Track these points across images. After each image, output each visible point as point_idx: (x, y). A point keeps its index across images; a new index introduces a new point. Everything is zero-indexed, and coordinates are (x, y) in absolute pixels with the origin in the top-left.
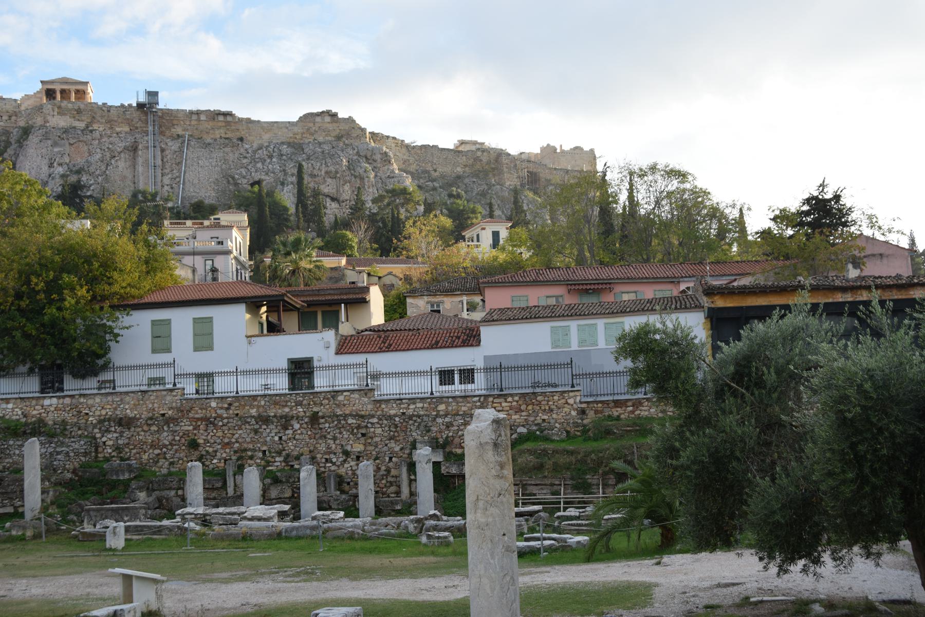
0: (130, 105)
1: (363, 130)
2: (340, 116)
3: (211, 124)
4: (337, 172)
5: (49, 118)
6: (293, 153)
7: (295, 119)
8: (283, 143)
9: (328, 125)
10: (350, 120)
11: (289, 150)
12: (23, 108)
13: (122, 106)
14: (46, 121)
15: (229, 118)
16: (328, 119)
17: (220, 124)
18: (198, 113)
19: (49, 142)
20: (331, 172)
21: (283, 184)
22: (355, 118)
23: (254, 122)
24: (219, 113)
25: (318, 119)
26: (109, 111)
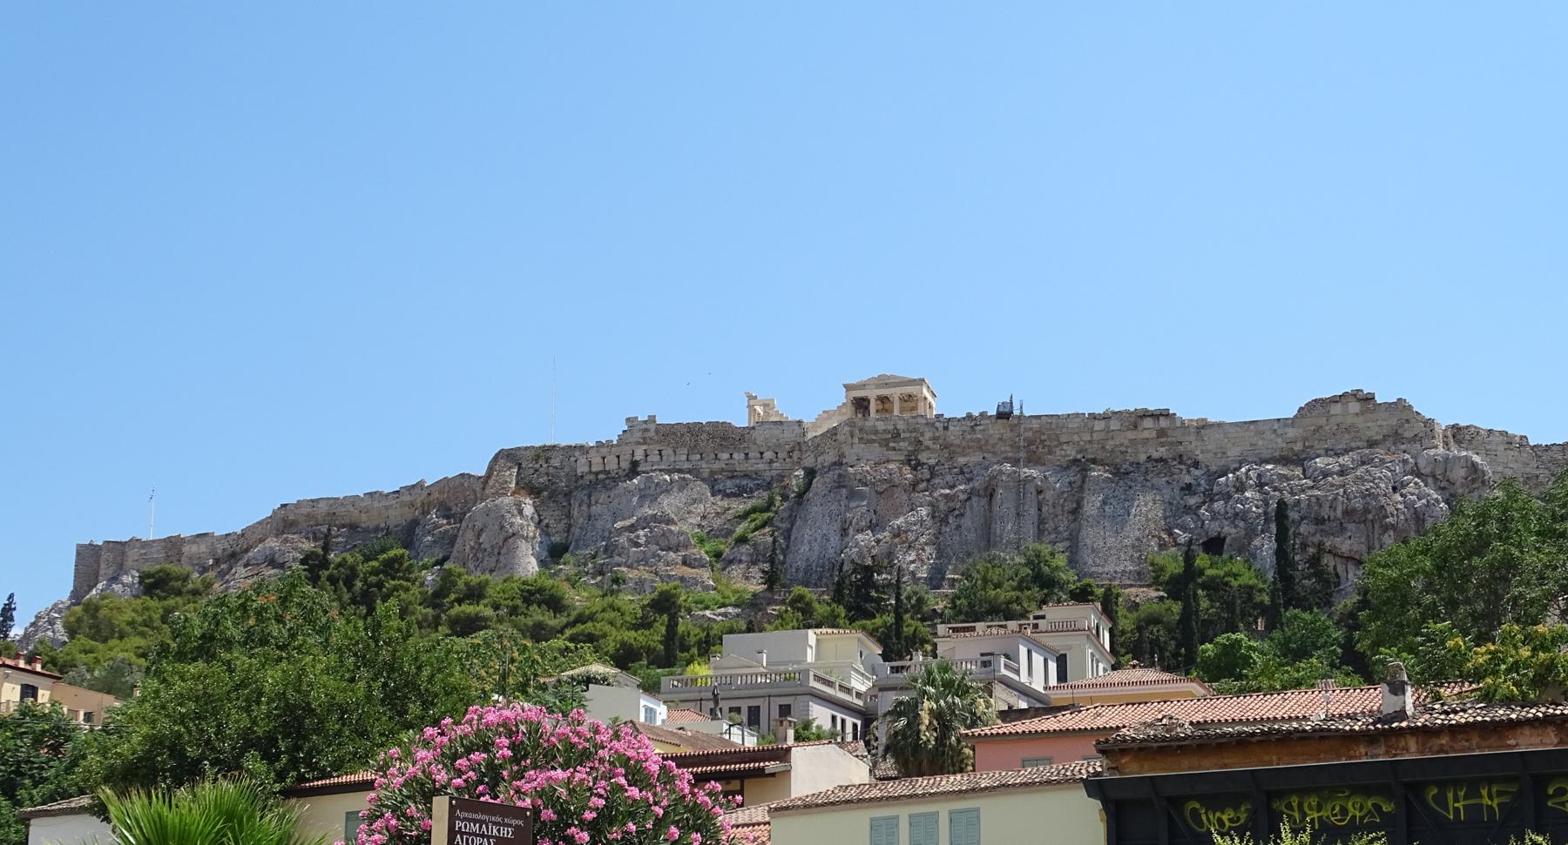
0: (983, 415)
1: (1429, 423)
3: (1131, 435)
4: (1366, 511)
5: (846, 450)
7: (1291, 413)
9: (1356, 420)
10: (1401, 406)
12: (810, 435)
13: (969, 416)
14: (842, 456)
15: (1163, 423)
16: (1354, 407)
17: (1146, 435)
18: (1106, 417)
19: (844, 491)
20: (1354, 510)
23: (1213, 425)
24: (1144, 415)
25: (1336, 409)
26: (946, 428)
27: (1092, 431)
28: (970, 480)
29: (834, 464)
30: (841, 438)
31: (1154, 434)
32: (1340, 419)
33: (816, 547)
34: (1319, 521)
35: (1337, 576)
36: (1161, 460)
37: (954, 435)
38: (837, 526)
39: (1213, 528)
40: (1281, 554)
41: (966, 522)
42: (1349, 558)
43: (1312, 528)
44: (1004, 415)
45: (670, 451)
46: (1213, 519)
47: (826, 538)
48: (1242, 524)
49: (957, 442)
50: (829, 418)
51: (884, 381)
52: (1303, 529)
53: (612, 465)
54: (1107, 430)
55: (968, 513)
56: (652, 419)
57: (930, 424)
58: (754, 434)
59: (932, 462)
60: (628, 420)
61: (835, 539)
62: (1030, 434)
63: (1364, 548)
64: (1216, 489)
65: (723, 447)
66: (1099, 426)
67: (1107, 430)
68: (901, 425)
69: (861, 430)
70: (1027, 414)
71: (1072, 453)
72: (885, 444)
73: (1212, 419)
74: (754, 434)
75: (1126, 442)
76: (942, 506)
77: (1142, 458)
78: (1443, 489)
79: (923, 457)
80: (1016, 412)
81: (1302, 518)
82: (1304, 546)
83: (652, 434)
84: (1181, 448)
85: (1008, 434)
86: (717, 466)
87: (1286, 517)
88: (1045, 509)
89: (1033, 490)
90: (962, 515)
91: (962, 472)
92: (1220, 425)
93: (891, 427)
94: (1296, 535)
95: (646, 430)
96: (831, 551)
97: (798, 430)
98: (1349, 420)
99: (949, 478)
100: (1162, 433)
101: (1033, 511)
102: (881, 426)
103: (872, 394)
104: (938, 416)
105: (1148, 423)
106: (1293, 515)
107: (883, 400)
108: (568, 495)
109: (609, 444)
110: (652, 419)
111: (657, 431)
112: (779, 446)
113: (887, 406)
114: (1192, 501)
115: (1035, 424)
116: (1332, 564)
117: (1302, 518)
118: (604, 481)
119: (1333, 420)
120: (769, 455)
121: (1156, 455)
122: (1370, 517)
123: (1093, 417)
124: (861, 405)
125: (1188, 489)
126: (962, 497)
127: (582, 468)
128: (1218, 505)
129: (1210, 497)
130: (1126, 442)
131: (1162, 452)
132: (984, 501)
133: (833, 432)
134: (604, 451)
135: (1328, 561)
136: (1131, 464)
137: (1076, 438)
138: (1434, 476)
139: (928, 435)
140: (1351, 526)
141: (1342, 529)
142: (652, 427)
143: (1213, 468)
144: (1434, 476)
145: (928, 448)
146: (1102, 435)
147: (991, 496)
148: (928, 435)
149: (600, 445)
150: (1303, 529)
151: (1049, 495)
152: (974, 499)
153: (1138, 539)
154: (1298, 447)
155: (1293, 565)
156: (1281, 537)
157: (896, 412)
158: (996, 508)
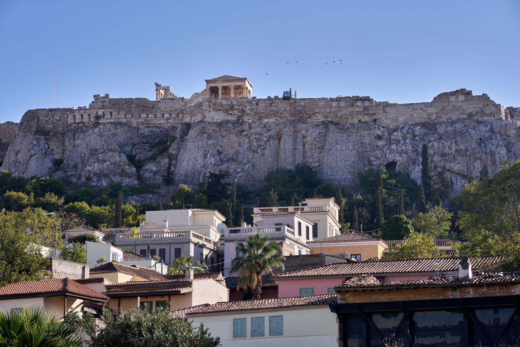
0: (276, 98)
1: (498, 107)
2: (474, 94)
3: (350, 109)
4: (467, 150)
5: (207, 114)
6: (426, 134)
7: (430, 100)
8: (417, 124)
9: (462, 104)
11: (423, 131)
13: (269, 98)
14: (204, 117)
15: (367, 104)
16: (461, 98)
17: (358, 109)
18: (338, 99)
19: (205, 135)
20: (461, 150)
21: (414, 163)
22: (489, 95)
23: (391, 105)
24: (357, 99)
25: (452, 98)
26: (257, 104)
27: (331, 107)
28: (269, 131)
29: (199, 122)
30: (204, 108)
31: (362, 109)
32: (454, 104)
33: (191, 164)
34: (443, 155)
35: (452, 183)
36: (366, 122)
37: (261, 107)
38: (201, 153)
39: (391, 157)
40: (425, 172)
41: (267, 152)
42: (458, 174)
43: (440, 158)
44: (287, 97)
45: (116, 113)
46: (390, 153)
47: (196, 159)
48: (405, 156)
49: (263, 111)
50: (198, 97)
51: (226, 79)
52: (436, 158)
53: (86, 119)
54: (339, 107)
55: (268, 148)
56: (107, 96)
57: (250, 102)
58: (160, 105)
59: (250, 121)
60: (95, 96)
61: (200, 160)
62: (300, 108)
63: (465, 169)
64: (392, 138)
65: (143, 111)
66: (334, 104)
67: (339, 107)
68: (234, 102)
69: (214, 104)
70: (298, 97)
71: (320, 118)
72: (226, 111)
73: (390, 102)
74: (160, 105)
75: (348, 113)
76: (255, 144)
77: (356, 121)
78: (504, 139)
79: (245, 119)
80: (293, 97)
81: (435, 153)
82: (436, 167)
83: (107, 104)
84: (376, 117)
85: (288, 108)
86: (140, 120)
87: (427, 153)
88: (307, 146)
89: (301, 136)
90: (265, 148)
91: (265, 126)
92: (395, 105)
93: (229, 103)
94: (432, 162)
95: (104, 102)
96: (198, 166)
97: (182, 103)
98: (459, 104)
99: (259, 130)
100: (366, 108)
101: (300, 147)
102: (224, 102)
103: (220, 85)
104: (254, 98)
105: (359, 103)
106: (430, 151)
107: (225, 88)
108: (63, 134)
109: (84, 109)
110: (107, 96)
111: (110, 102)
112: (172, 111)
113: (228, 91)
114: (381, 143)
115: (302, 104)
116: (449, 177)
117: (435, 153)
118: (80, 129)
119: (451, 104)
120: (167, 116)
121: (363, 120)
122: (468, 153)
123: (332, 100)
124: (214, 91)
125: (380, 138)
126: (265, 139)
127: (70, 120)
128: (394, 147)
129: (390, 142)
130: (348, 113)
131: (366, 118)
132: (276, 142)
133: (200, 105)
134: (82, 112)
135: (448, 175)
136: (350, 124)
137: (323, 110)
138: (500, 133)
139: (248, 108)
140: (459, 158)
141: (455, 159)
142: (107, 100)
143: (391, 127)
144: (500, 133)
145: (248, 114)
146: (336, 109)
147: (280, 139)
148: (248, 108)
149: (80, 109)
150: (436, 158)
151: (308, 139)
152: (271, 140)
153: (353, 162)
154: (434, 117)
155: (430, 178)
156: (425, 163)
157: (232, 95)
158: (282, 145)
